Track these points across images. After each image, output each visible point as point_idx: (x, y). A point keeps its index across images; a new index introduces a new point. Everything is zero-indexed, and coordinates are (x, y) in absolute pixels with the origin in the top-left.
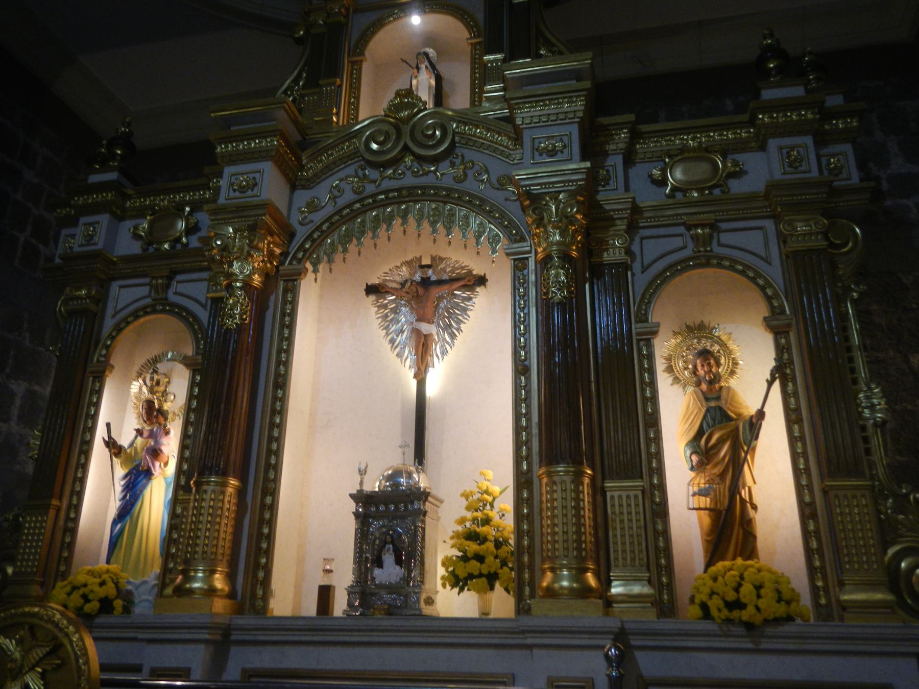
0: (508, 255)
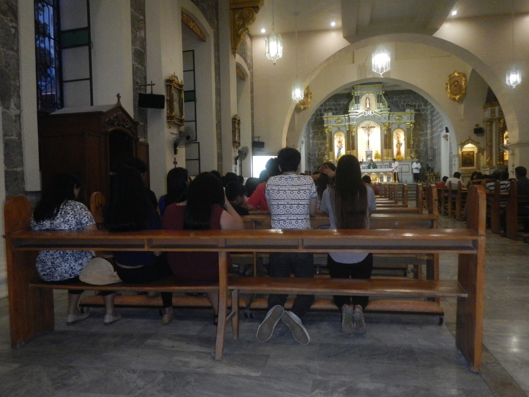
0: (380, 127)
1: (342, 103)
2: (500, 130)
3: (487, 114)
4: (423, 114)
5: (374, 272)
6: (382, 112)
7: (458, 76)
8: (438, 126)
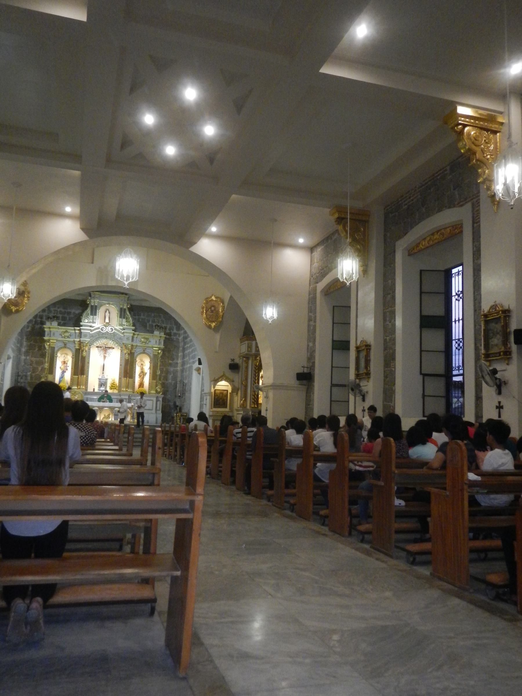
1: (73, 311)
2: (256, 369)
3: (244, 349)
4: (175, 339)
5: (68, 546)
6: (124, 331)
7: (216, 301)
8: (191, 355)
